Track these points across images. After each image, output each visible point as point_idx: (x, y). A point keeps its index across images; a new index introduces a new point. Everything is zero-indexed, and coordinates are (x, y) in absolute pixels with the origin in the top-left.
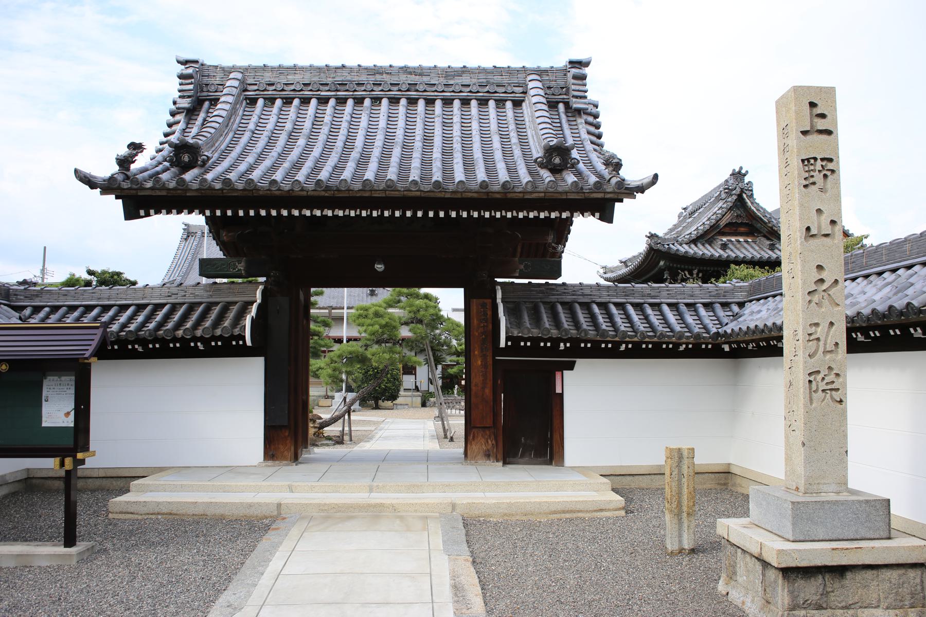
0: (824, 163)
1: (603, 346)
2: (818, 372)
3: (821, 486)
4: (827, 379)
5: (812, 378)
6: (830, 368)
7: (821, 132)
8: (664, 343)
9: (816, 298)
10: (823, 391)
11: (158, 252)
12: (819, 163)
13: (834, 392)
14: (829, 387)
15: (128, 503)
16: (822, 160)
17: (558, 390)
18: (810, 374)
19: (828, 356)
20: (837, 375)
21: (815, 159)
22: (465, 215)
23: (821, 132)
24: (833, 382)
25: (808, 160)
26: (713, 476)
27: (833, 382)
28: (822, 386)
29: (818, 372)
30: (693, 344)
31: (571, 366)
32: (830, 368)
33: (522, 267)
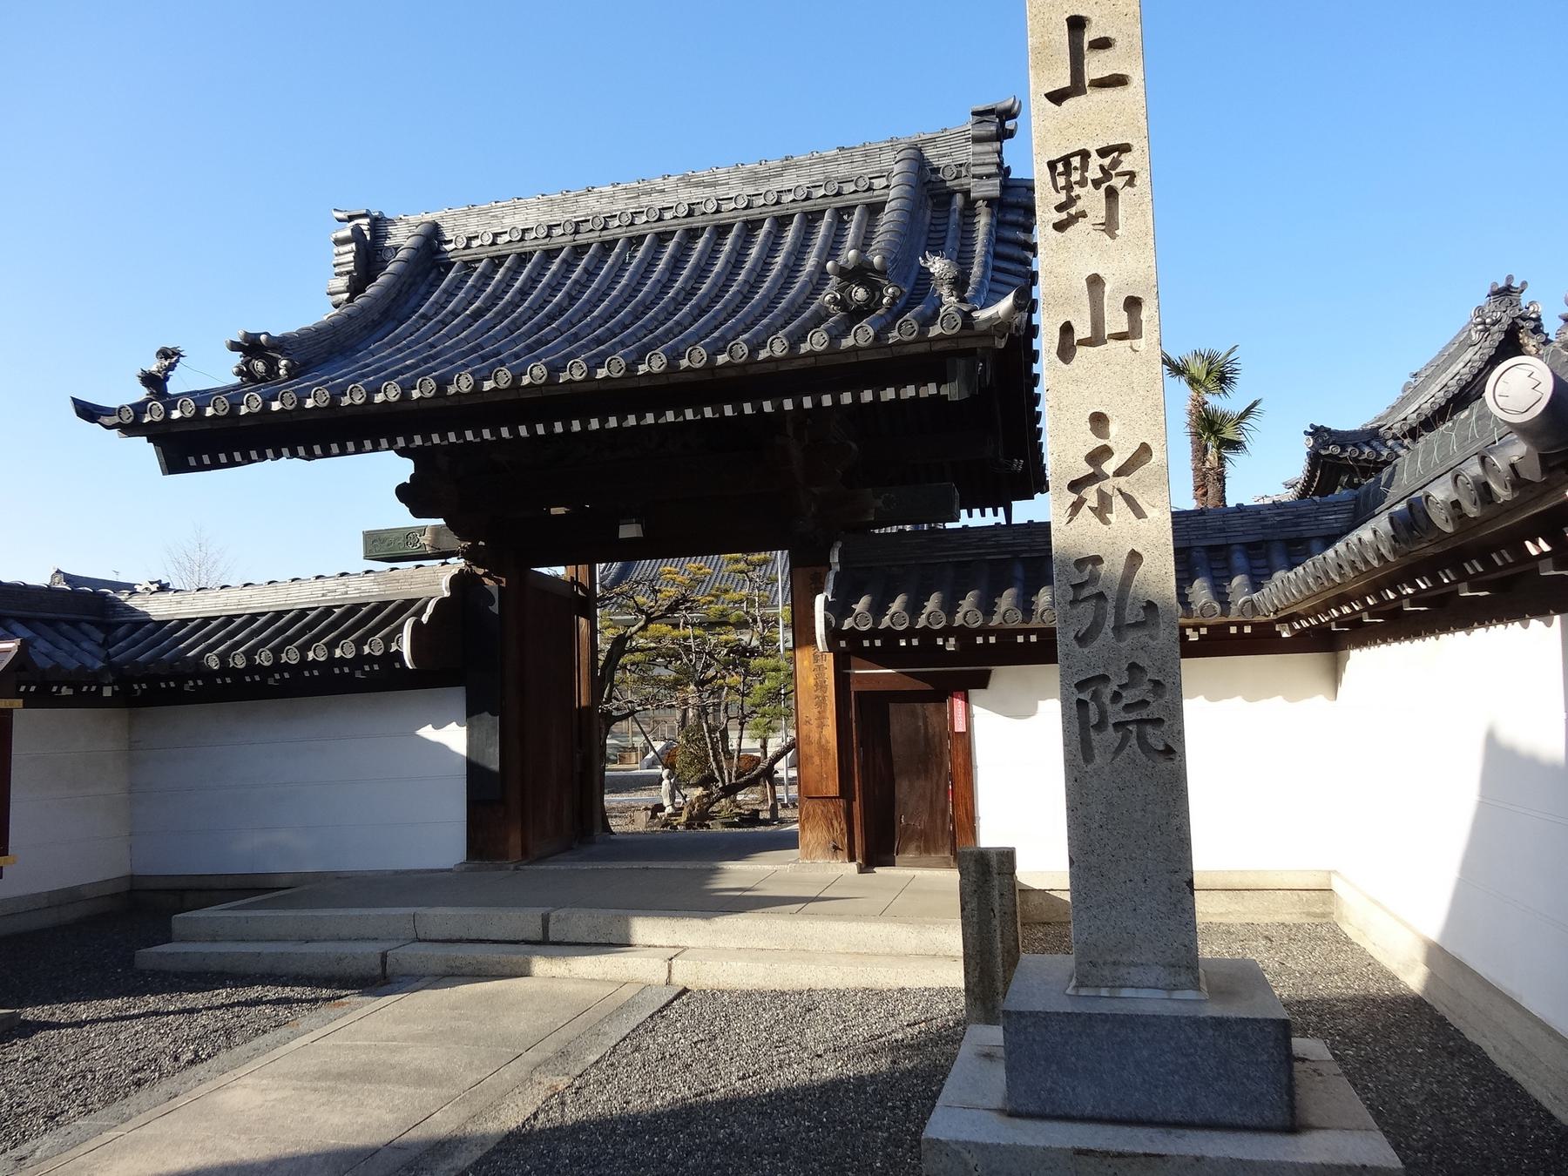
0: (1107, 161)
1: (980, 640)
2: (1104, 679)
3: (1123, 971)
4: (1129, 697)
5: (1085, 696)
6: (1134, 668)
7: (1101, 84)
8: (1233, 623)
9: (1091, 495)
10: (1117, 726)
11: (319, 533)
12: (1095, 161)
13: (1149, 729)
14: (1133, 716)
15: (161, 955)
16: (1103, 153)
17: (960, 727)
18: (1081, 686)
19: (1131, 637)
20: (1157, 684)
21: (1085, 155)
22: (708, 412)
23: (1101, 84)
24: (1144, 703)
25: (1066, 160)
26: (1294, 896)
27: (1144, 703)
28: (1116, 714)
29: (1104, 679)
30: (1253, 625)
31: (982, 682)
32: (1134, 668)
33: (879, 503)
